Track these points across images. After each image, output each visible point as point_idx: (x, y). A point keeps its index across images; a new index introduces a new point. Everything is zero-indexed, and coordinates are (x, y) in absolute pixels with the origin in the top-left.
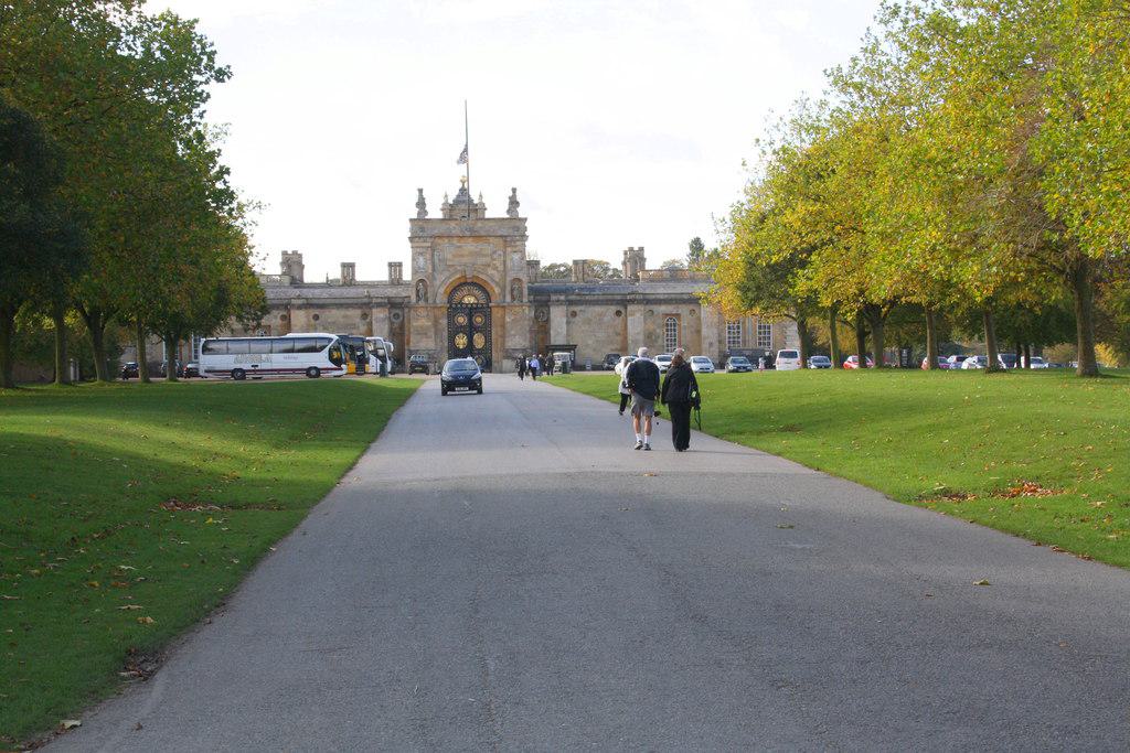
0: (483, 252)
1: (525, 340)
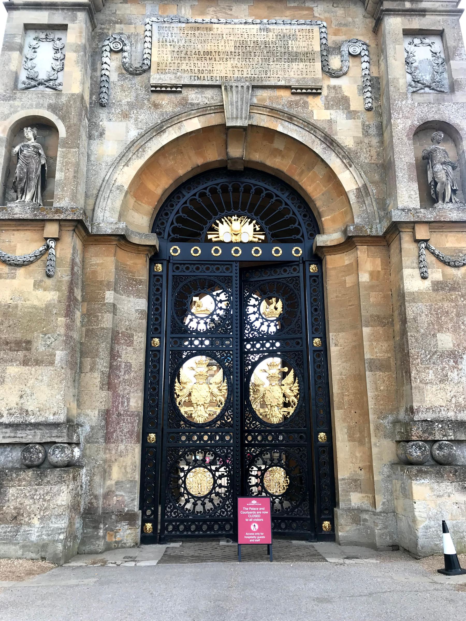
0: (294, 46)
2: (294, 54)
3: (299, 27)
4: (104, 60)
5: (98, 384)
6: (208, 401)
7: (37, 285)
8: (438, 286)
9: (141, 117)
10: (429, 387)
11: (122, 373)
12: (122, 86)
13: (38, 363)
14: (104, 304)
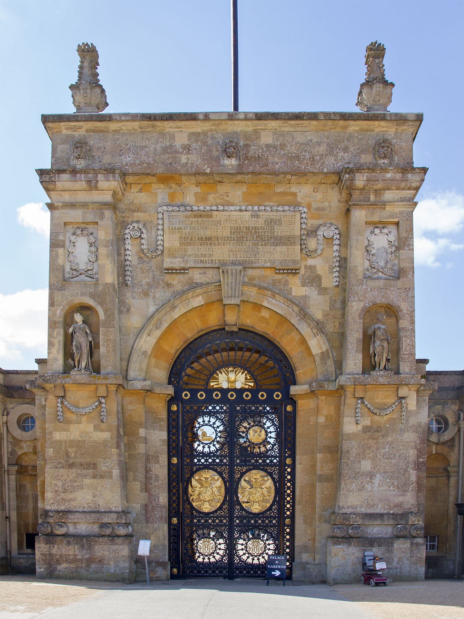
0: (279, 231)
3: (284, 213)
8: (366, 429)
9: (157, 295)
12: (142, 268)
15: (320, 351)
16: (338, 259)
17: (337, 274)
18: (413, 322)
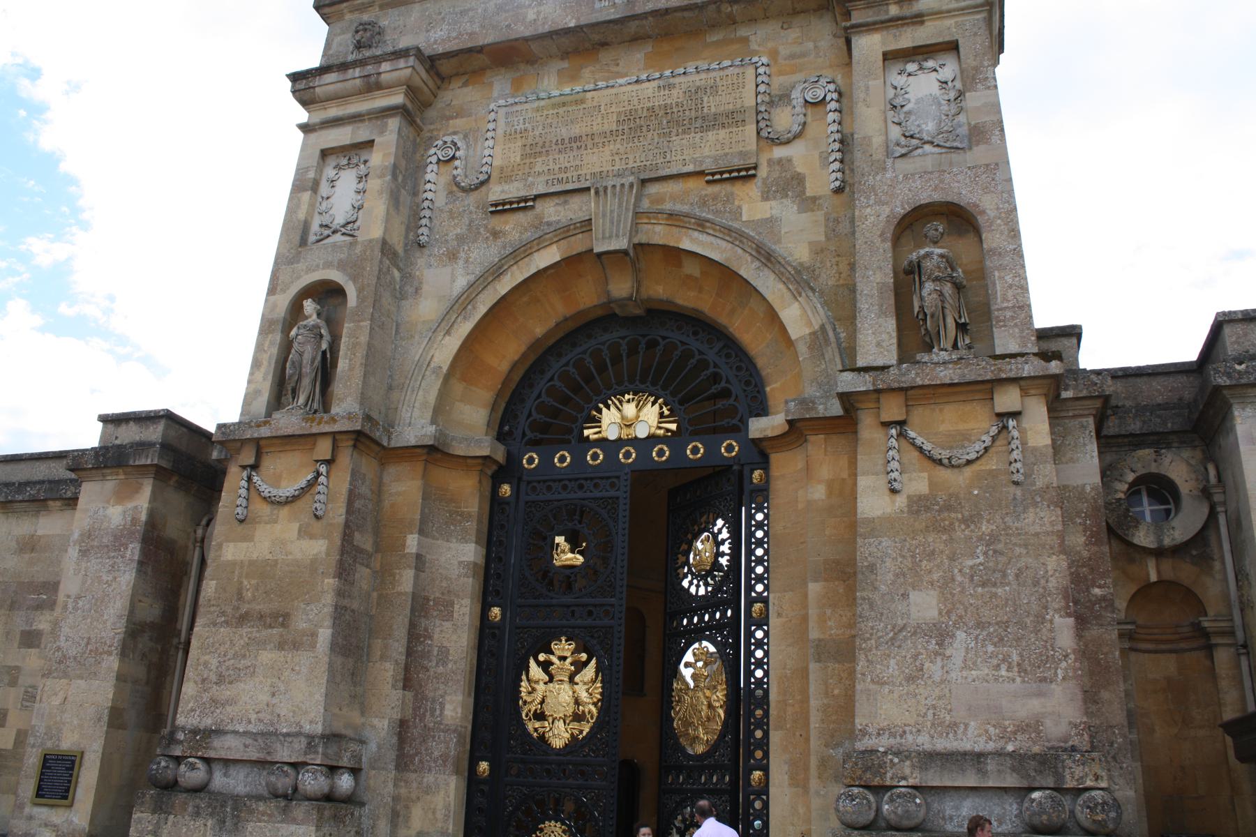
0: (712, 105)
1: (1036, 669)
2: (711, 118)
3: (721, 73)
4: (428, 177)
5: (390, 680)
6: (570, 712)
7: (304, 533)
8: (918, 505)
10: (886, 689)
11: (434, 664)
12: (451, 211)
13: (296, 646)
14: (404, 555)
15: (807, 331)
16: (838, 136)
17: (837, 165)
18: (1015, 234)
